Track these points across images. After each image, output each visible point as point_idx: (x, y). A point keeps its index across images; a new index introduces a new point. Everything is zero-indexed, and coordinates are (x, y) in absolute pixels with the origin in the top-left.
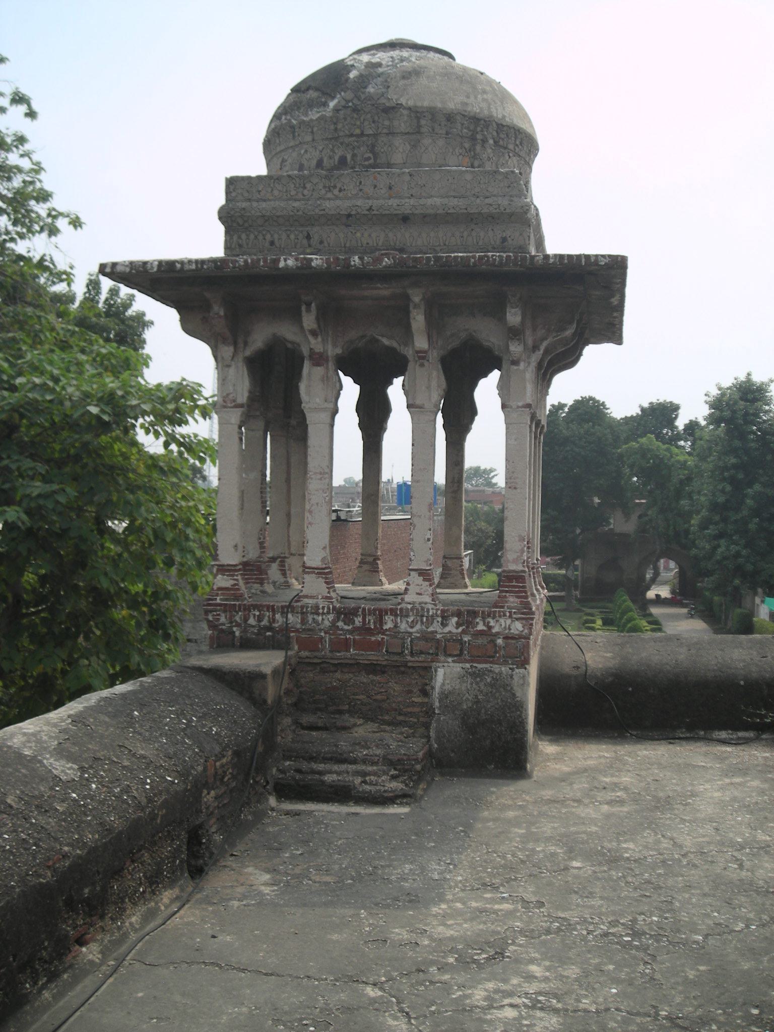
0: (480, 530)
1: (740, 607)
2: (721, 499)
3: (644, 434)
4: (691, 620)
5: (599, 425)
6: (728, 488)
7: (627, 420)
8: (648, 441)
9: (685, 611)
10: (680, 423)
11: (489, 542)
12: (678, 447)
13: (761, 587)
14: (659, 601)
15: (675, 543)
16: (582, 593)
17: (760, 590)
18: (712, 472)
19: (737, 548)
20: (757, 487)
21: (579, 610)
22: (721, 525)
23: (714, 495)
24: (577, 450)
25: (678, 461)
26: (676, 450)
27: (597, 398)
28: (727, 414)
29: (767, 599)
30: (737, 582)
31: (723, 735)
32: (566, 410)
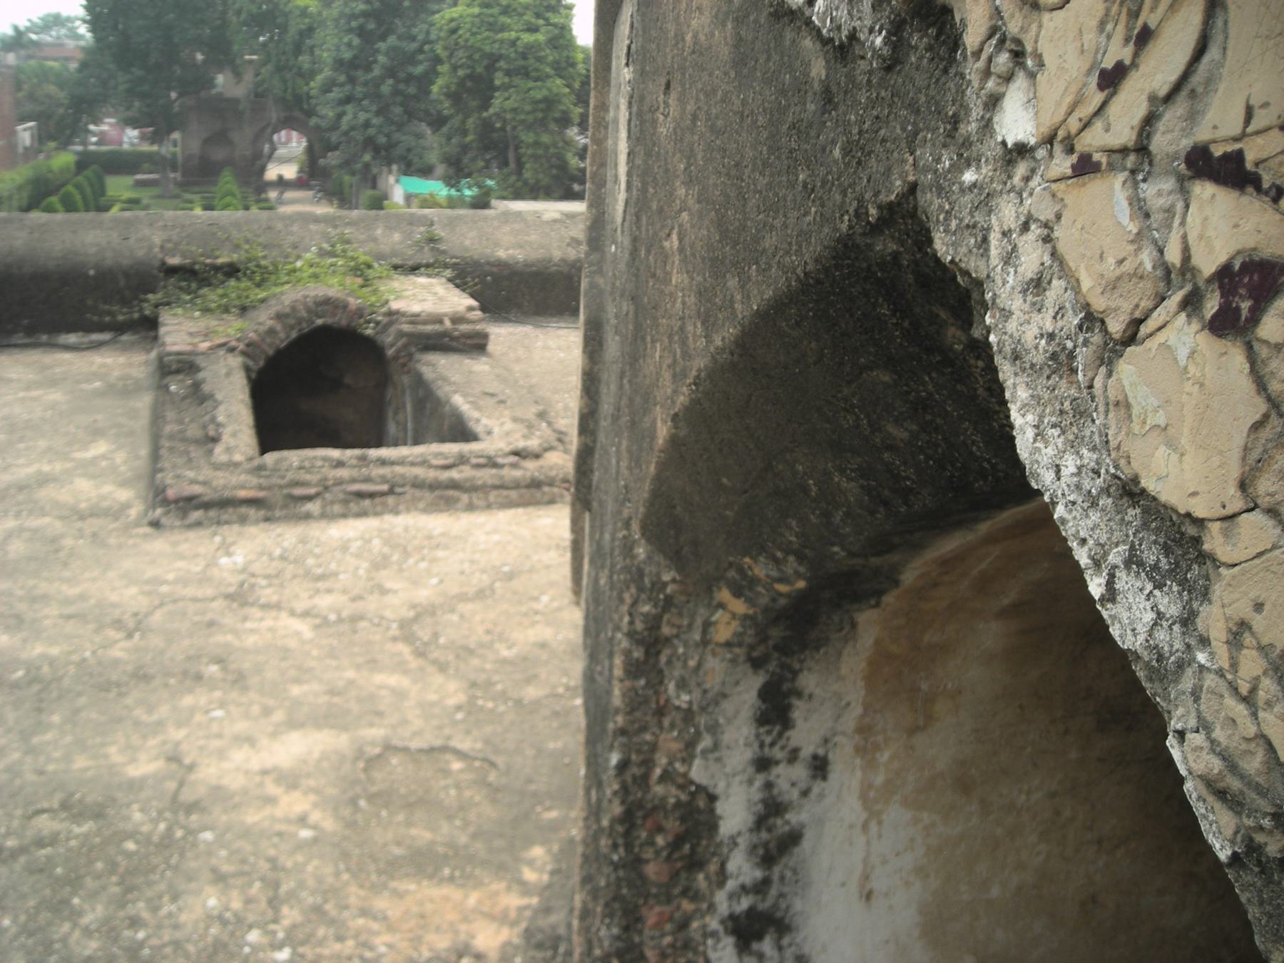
0: (49, 97)
2: (347, 55)
9: (311, 193)
11: (61, 111)
14: (281, 183)
15: (296, 112)
16: (184, 175)
17: (395, 167)
18: (336, 20)
20: (392, 40)
21: (177, 197)
22: (348, 88)
23: (338, 50)
29: (405, 179)
30: (367, 157)
31: (72, 338)
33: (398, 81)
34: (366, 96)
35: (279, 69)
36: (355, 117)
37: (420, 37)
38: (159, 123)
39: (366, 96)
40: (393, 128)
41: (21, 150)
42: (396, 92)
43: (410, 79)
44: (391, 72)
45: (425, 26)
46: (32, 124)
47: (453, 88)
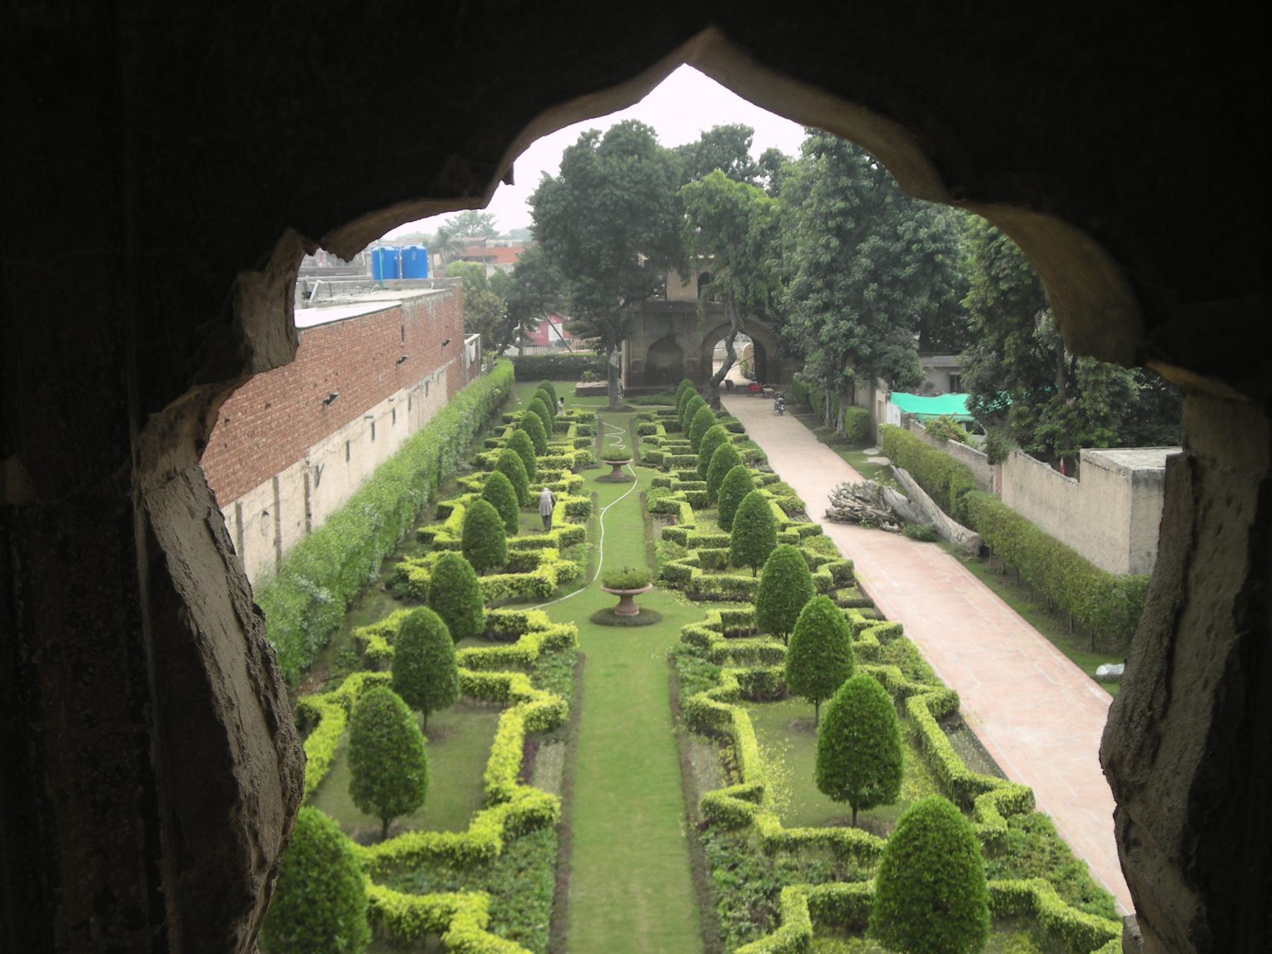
0: (487, 303)
1: (853, 404)
2: (825, 258)
3: (711, 170)
5: (647, 158)
6: (835, 243)
7: (683, 151)
8: (716, 178)
9: (770, 403)
10: (755, 153)
11: (499, 319)
12: (755, 184)
13: (882, 376)
16: (628, 382)
18: (811, 220)
19: (849, 324)
20: (874, 241)
22: (826, 293)
23: (814, 251)
24: (618, 193)
25: (758, 205)
27: (643, 122)
32: (601, 138)
33: (881, 285)
34: (846, 302)
35: (737, 273)
37: (908, 236)
38: (606, 332)
39: (846, 302)
40: (877, 337)
41: (468, 365)
42: (880, 297)
43: (895, 282)
44: (874, 276)
45: (912, 224)
46: (476, 336)
47: (990, 303)
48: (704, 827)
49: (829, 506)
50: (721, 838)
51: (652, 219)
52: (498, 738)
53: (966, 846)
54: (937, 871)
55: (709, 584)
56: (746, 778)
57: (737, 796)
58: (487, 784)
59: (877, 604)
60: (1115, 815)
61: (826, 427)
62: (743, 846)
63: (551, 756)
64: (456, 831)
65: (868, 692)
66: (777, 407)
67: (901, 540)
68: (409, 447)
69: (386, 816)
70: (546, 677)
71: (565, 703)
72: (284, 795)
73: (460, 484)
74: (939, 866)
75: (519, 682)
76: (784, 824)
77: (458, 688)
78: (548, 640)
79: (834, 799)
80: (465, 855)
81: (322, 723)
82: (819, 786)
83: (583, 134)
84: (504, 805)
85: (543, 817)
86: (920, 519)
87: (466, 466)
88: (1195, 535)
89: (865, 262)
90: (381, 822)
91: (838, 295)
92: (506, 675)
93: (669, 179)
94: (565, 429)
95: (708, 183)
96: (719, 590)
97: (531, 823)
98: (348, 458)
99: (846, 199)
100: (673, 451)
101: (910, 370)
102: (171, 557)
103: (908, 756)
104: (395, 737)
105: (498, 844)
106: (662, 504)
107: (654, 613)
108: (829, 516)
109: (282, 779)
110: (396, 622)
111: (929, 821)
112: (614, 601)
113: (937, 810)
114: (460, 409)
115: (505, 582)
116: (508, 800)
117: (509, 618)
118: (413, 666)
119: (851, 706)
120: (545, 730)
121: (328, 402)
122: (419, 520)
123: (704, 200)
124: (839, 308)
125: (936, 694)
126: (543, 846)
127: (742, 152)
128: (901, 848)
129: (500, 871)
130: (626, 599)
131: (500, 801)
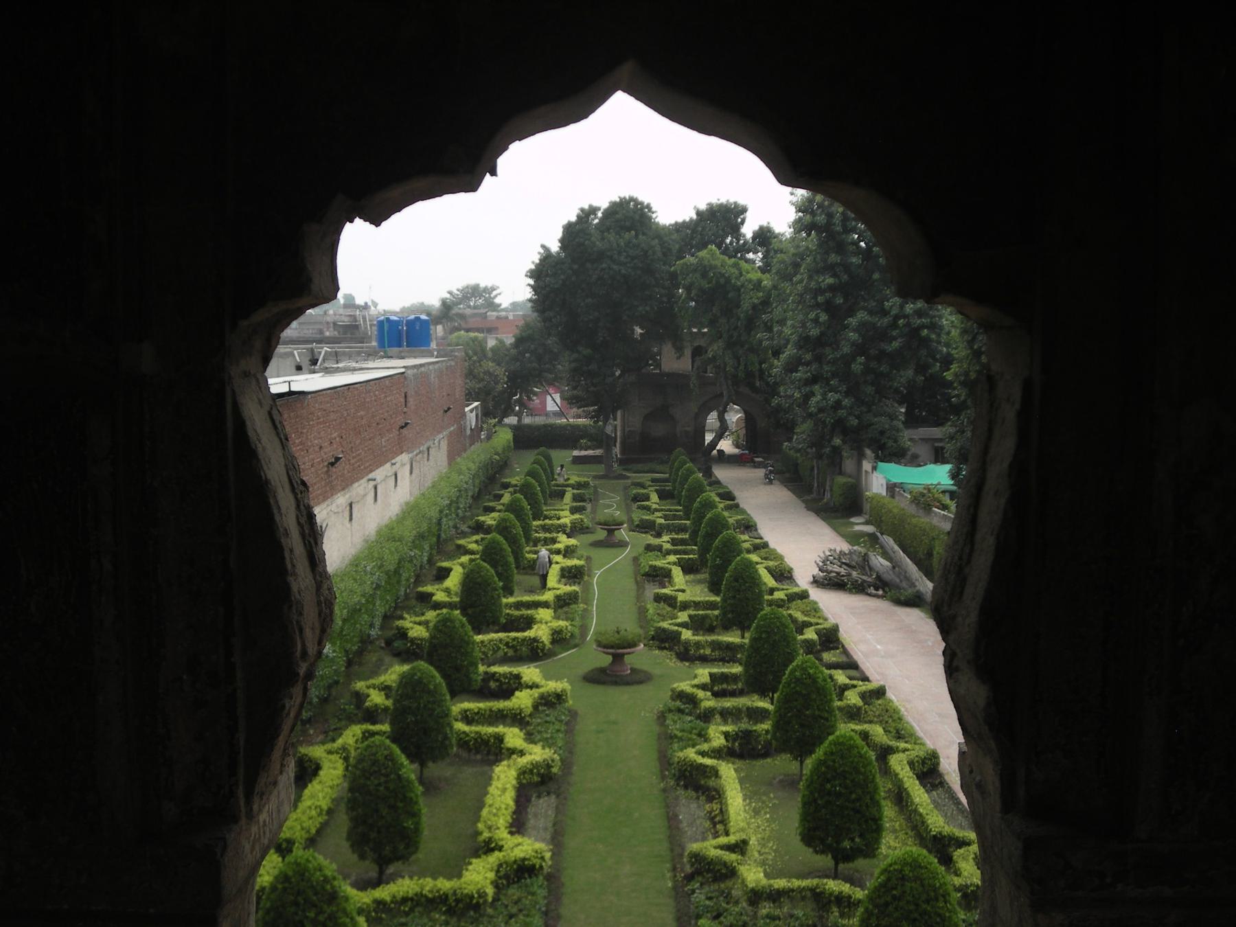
0: (490, 374)
1: (841, 473)
2: (815, 332)
4: (768, 487)
5: (644, 234)
6: (823, 317)
8: (710, 253)
9: (761, 472)
10: (748, 230)
11: (499, 388)
12: (747, 261)
16: (623, 451)
17: (868, 452)
18: (801, 295)
19: (837, 396)
20: (862, 315)
23: (804, 325)
24: (615, 267)
25: (750, 281)
26: (743, 264)
27: (640, 199)
28: (821, 219)
29: (880, 464)
32: (600, 214)
34: (834, 375)
36: (825, 399)
37: (893, 312)
40: (864, 409)
41: (468, 432)
44: (860, 349)
46: (476, 404)
47: (973, 376)
48: (690, 878)
49: (816, 571)
50: (706, 889)
51: (647, 293)
52: (492, 789)
53: (943, 896)
54: (915, 920)
55: (698, 645)
56: (732, 830)
57: (722, 847)
58: (481, 833)
59: (861, 665)
60: (944, 653)
61: (814, 495)
62: (728, 897)
63: (543, 807)
64: (449, 878)
65: (851, 748)
66: (766, 476)
67: (884, 605)
68: (410, 510)
69: (383, 862)
70: (539, 732)
71: (556, 757)
72: (320, 615)
73: (459, 547)
74: (916, 915)
75: (513, 737)
76: (767, 875)
77: (454, 741)
78: (542, 697)
79: (816, 852)
80: (458, 901)
81: (321, 773)
82: (803, 840)
83: (582, 210)
84: (497, 853)
85: (534, 866)
86: (904, 584)
87: (464, 528)
88: (990, 431)
89: (853, 336)
90: (376, 868)
91: (826, 368)
92: (500, 729)
93: (664, 254)
94: (561, 495)
95: (702, 259)
96: (708, 651)
97: (521, 871)
98: (351, 519)
99: (835, 275)
100: (666, 517)
101: (896, 441)
102: (248, 423)
103: (889, 811)
104: (392, 786)
105: (490, 891)
106: (654, 568)
107: (645, 672)
108: (816, 582)
109: (319, 603)
110: (394, 677)
111: (907, 870)
112: (605, 660)
113: (915, 860)
114: (460, 473)
115: (501, 640)
116: (500, 849)
117: (504, 675)
118: (411, 718)
119: (834, 761)
120: (537, 782)
121: (332, 464)
122: (419, 580)
123: (698, 275)
124: (828, 380)
125: (917, 752)
126: (533, 894)
127: (735, 229)
128: (879, 897)
129: (492, 917)
130: (618, 658)
131: (492, 850)
